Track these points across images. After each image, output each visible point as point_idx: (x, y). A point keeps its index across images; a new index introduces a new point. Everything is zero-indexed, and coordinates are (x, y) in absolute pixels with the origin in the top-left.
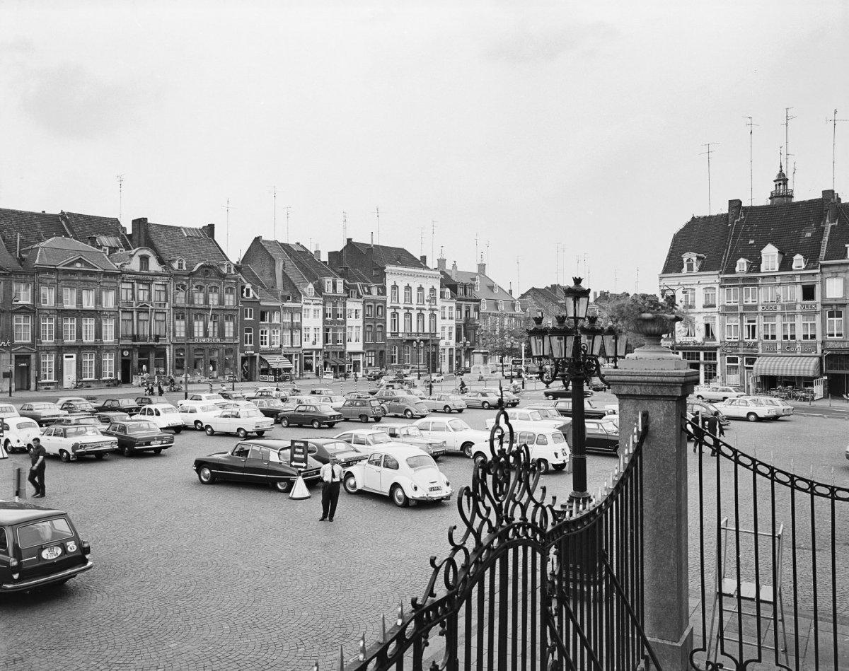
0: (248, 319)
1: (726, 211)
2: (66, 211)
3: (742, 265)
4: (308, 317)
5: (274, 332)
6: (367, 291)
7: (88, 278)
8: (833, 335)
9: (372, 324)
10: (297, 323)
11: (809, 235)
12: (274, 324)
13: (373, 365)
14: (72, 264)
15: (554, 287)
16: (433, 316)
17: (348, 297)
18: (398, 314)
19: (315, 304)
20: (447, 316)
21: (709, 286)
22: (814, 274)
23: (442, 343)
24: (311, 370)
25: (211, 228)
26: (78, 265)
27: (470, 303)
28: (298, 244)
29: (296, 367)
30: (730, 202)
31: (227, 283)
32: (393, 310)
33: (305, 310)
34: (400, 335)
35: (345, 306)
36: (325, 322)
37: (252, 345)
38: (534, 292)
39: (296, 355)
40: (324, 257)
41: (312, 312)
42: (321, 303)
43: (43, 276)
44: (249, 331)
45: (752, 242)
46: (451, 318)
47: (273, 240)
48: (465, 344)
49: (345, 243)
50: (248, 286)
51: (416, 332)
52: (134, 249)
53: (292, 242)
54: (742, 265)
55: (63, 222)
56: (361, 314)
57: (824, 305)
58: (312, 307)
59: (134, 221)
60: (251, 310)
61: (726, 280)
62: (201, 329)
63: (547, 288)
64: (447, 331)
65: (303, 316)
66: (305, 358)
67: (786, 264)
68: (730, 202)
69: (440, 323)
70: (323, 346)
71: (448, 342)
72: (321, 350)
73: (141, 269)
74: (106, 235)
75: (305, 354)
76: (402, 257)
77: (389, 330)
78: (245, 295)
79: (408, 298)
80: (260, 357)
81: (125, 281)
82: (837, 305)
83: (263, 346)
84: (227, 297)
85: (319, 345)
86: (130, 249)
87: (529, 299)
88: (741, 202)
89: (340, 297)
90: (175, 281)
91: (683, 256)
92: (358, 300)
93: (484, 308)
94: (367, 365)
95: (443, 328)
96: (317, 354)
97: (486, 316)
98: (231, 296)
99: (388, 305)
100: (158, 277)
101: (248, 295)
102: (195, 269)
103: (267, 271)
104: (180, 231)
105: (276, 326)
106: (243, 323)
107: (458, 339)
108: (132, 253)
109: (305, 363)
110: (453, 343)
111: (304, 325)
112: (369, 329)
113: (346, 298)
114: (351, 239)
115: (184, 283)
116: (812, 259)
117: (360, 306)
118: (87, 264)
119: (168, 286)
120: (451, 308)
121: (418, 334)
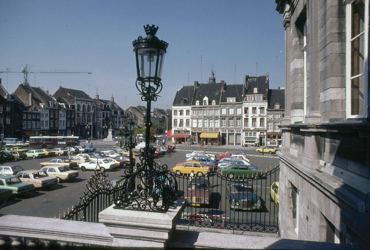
1: (193, 85)
3: (198, 102)
11: (217, 94)
30: (195, 82)
34: (81, 124)
49: (59, 88)
54: (198, 102)
57: (221, 116)
61: (193, 107)
67: (210, 103)
68: (195, 82)
88: (198, 82)
111: (41, 120)
113: (59, 110)
114: (61, 87)
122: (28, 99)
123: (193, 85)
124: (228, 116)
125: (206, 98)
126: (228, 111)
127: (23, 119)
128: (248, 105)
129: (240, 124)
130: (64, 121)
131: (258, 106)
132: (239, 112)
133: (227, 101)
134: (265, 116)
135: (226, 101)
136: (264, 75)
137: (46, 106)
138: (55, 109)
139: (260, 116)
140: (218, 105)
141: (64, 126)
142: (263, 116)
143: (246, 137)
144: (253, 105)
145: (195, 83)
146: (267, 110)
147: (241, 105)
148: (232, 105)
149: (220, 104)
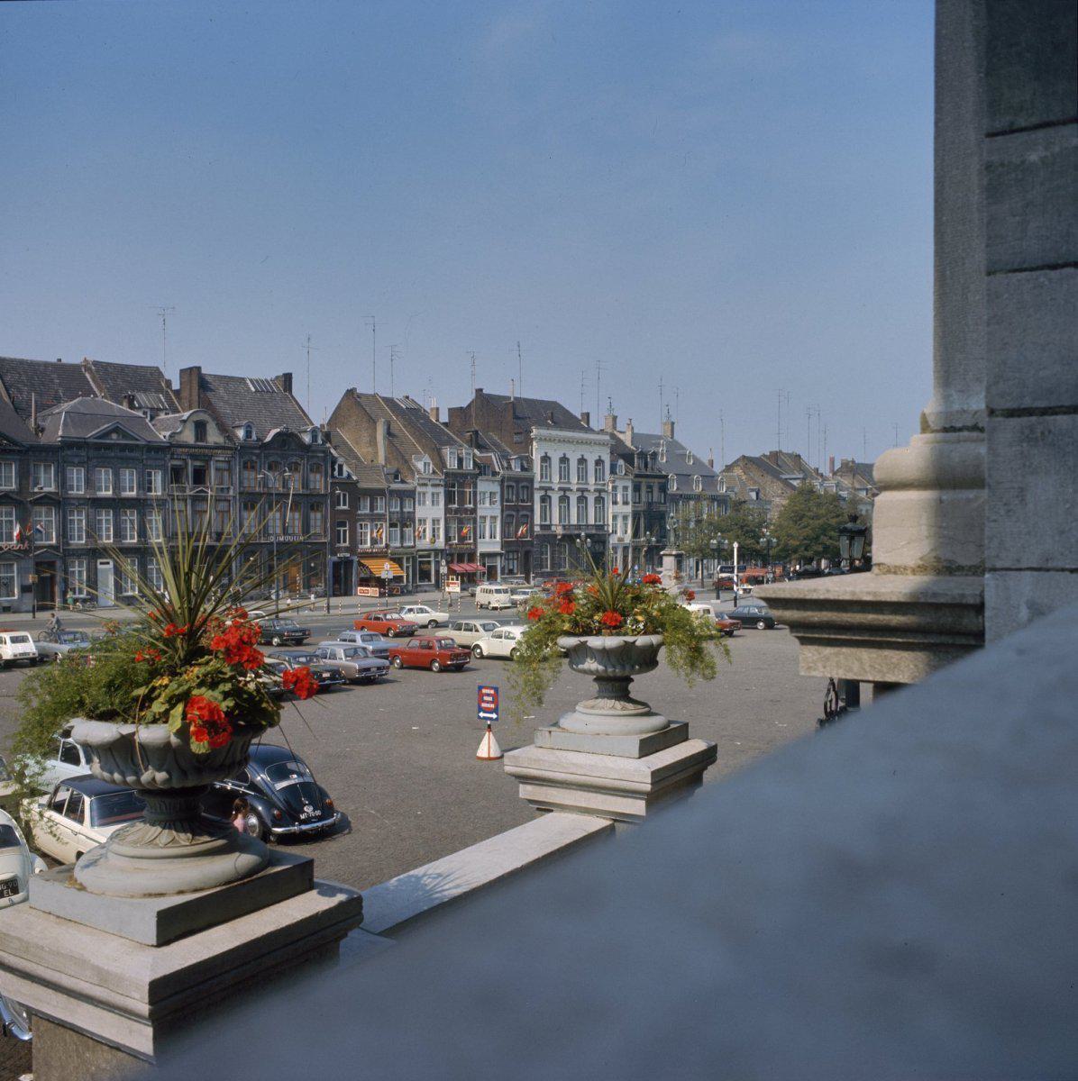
0: (342, 507)
2: (91, 359)
4: (424, 503)
5: (377, 525)
6: (505, 465)
7: (127, 453)
9: (514, 513)
10: (409, 512)
12: (378, 514)
13: (515, 571)
14: (106, 434)
15: (775, 456)
16: (599, 500)
17: (480, 474)
18: (550, 497)
19: (433, 485)
20: (619, 498)
23: (613, 540)
24: (430, 580)
25: (287, 379)
26: (114, 436)
27: (653, 480)
28: (407, 397)
29: (408, 576)
31: (313, 457)
32: (543, 493)
33: (419, 493)
35: (475, 487)
36: (447, 511)
37: (347, 544)
38: (747, 462)
39: (408, 559)
40: (444, 418)
41: (429, 497)
42: (442, 483)
43: (69, 453)
44: (343, 524)
46: (625, 503)
47: (371, 392)
48: (649, 541)
49: (474, 396)
50: (341, 460)
51: (575, 523)
52: (184, 410)
53: (397, 395)
55: (88, 375)
56: (498, 498)
58: (430, 490)
59: (181, 371)
60: (344, 496)
62: (278, 523)
63: (764, 455)
65: (417, 503)
66: (420, 562)
69: (611, 510)
70: (445, 545)
71: (621, 533)
72: (442, 551)
73: (197, 439)
74: (145, 391)
75: (420, 557)
76: (555, 416)
77: (537, 520)
78: (336, 473)
79: (564, 474)
80: (359, 562)
81: (175, 457)
83: (366, 546)
84: (312, 476)
85: (441, 543)
86: (179, 412)
87: (738, 471)
89: (468, 474)
90: (241, 457)
92: (493, 478)
93: (674, 488)
94: (506, 571)
95: (615, 518)
96: (436, 556)
97: (675, 499)
98: (318, 476)
99: (536, 485)
100: (220, 451)
101: (341, 472)
102: (268, 439)
103: (365, 439)
104: (245, 383)
105: (381, 517)
106: (335, 513)
107: (636, 534)
108: (185, 418)
109: (421, 570)
110: (628, 538)
111: (418, 516)
112: (509, 520)
113: (476, 476)
114: (481, 390)
115: (254, 458)
117: (496, 488)
118: (125, 435)
119: (232, 463)
120: (625, 488)
121: (578, 527)
122: (373, 442)
127: (361, 515)
130: (494, 518)
137: (431, 465)
138: (464, 476)
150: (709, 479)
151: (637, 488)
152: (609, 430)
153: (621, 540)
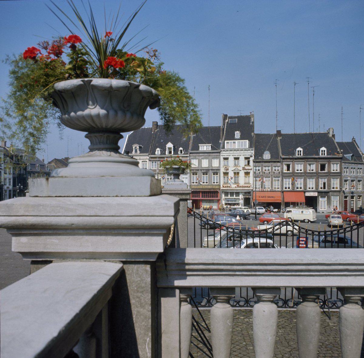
1: (151, 126)
3: (158, 151)
8: (194, 183)
11: (184, 139)
20: (7, 172)
21: (144, 160)
22: (187, 157)
45: (162, 141)
48: (20, 187)
61: (152, 157)
64: (7, 181)
82: (196, 170)
87: (53, 164)
88: (157, 123)
91: (133, 146)
93: (29, 169)
95: (5, 179)
107: (14, 185)
110: (11, 187)
116: (186, 149)
123: (151, 126)
124: (201, 170)
125: (170, 145)
126: (200, 163)
128: (239, 154)
129: (217, 180)
131: (241, 155)
132: (215, 163)
133: (200, 149)
134: (251, 169)
135: (198, 148)
136: (249, 114)
139: (244, 169)
140: (187, 154)
141: (10, 185)
142: (249, 169)
143: (225, 199)
144: (246, 154)
145: (153, 123)
146: (254, 162)
147: (218, 154)
148: (206, 154)
149: (190, 153)
150: (43, 166)
151: (14, 169)
152: (4, 146)
153: (8, 188)
